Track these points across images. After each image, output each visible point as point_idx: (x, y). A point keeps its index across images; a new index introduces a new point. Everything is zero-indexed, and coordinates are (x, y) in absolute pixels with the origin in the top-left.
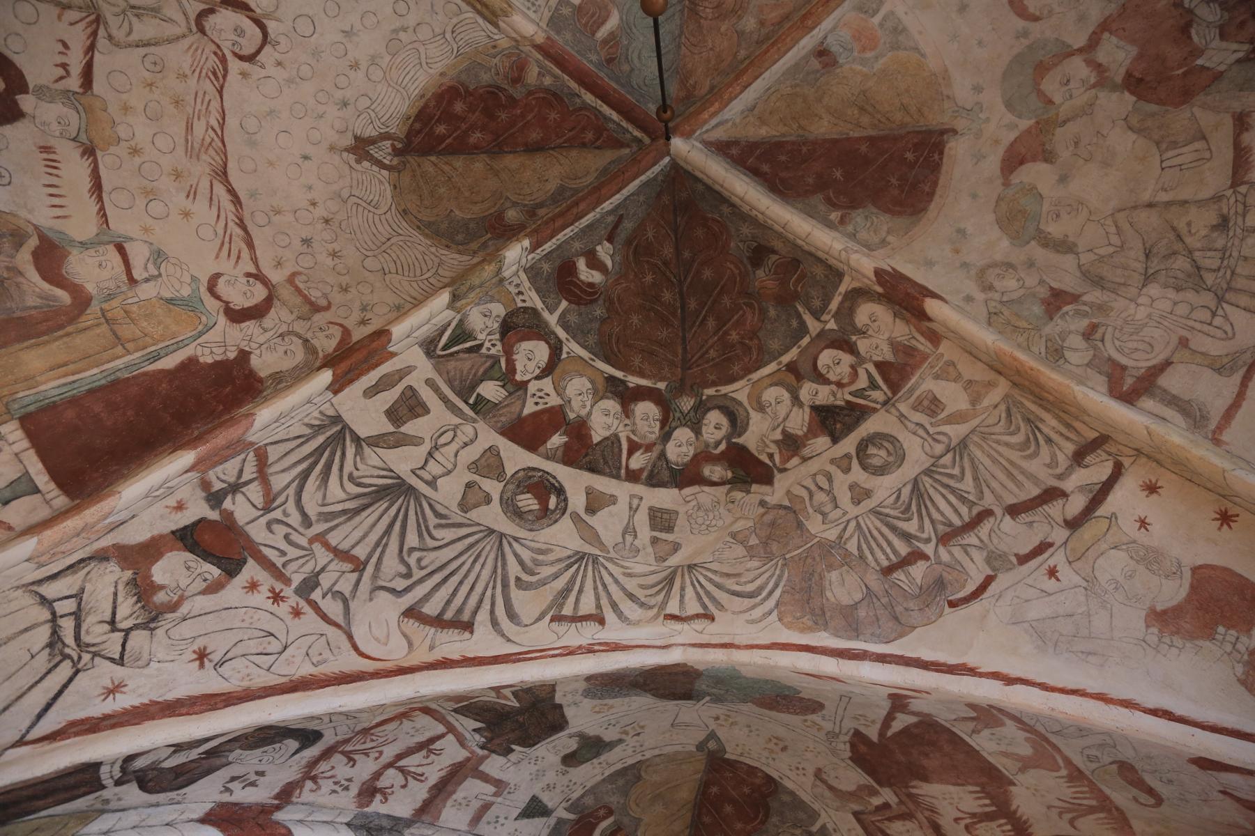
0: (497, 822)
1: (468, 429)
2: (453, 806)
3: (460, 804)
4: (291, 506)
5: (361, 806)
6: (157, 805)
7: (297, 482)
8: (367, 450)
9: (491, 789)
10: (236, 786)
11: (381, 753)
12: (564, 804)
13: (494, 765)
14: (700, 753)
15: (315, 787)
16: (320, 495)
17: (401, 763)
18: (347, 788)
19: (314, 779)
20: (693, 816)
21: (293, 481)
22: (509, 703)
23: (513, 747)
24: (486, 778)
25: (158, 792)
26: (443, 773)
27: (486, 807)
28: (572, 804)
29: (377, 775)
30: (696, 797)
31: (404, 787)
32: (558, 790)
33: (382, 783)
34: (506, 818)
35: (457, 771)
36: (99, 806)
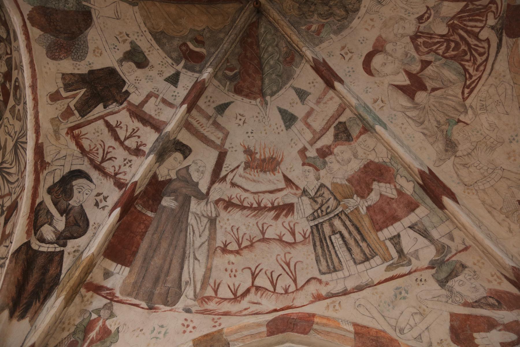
0: (176, 96)
1: (6, 120)
2: (159, 116)
3: (159, 113)
4: (13, 186)
5: (144, 155)
6: (95, 234)
7: (9, 185)
8: (5, 159)
9: (153, 100)
10: (101, 205)
11: (109, 147)
12: (174, 66)
13: (135, 99)
14: (139, 4)
15: (124, 174)
16: (14, 175)
17: (122, 138)
18: (130, 161)
19: (116, 174)
20: (187, 4)
21: (8, 185)
22: (82, 93)
23: (124, 90)
24: (145, 101)
25: (86, 233)
26: (136, 121)
27: (164, 101)
28: (175, 62)
29: (127, 148)
30: (173, 3)
31: (139, 137)
32: (164, 69)
33: (133, 146)
34: (174, 92)
35: (136, 114)
36: (77, 254)
